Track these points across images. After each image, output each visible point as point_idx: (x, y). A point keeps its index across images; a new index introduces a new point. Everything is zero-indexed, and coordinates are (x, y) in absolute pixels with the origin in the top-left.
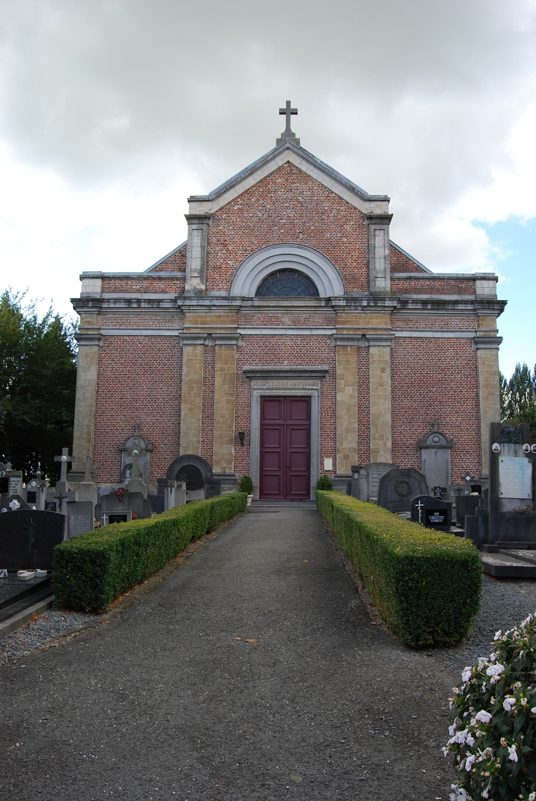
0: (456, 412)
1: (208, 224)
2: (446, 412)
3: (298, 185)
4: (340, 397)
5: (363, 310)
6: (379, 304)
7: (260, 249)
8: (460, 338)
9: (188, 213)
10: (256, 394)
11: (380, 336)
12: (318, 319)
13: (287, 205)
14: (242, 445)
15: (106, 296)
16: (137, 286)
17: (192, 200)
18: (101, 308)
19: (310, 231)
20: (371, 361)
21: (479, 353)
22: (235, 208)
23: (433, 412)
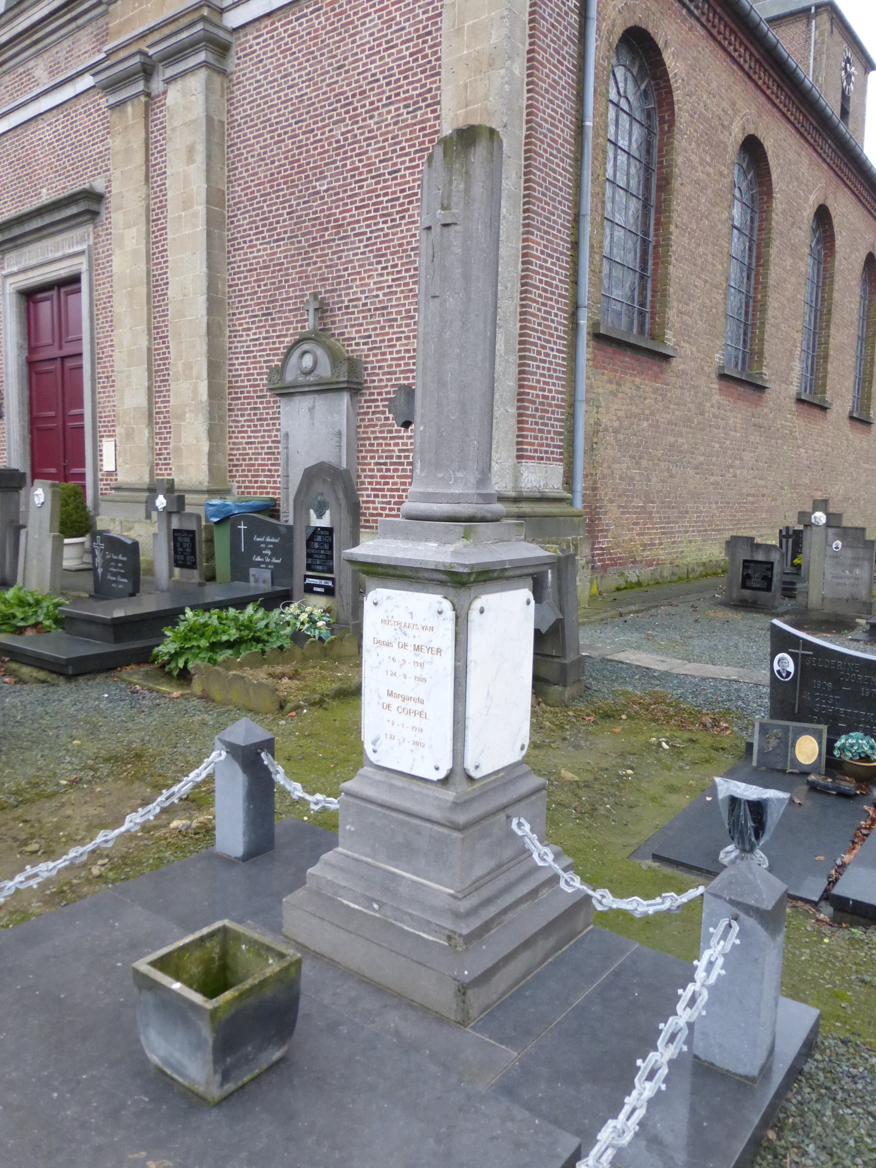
2: (352, 261)
23: (320, 268)
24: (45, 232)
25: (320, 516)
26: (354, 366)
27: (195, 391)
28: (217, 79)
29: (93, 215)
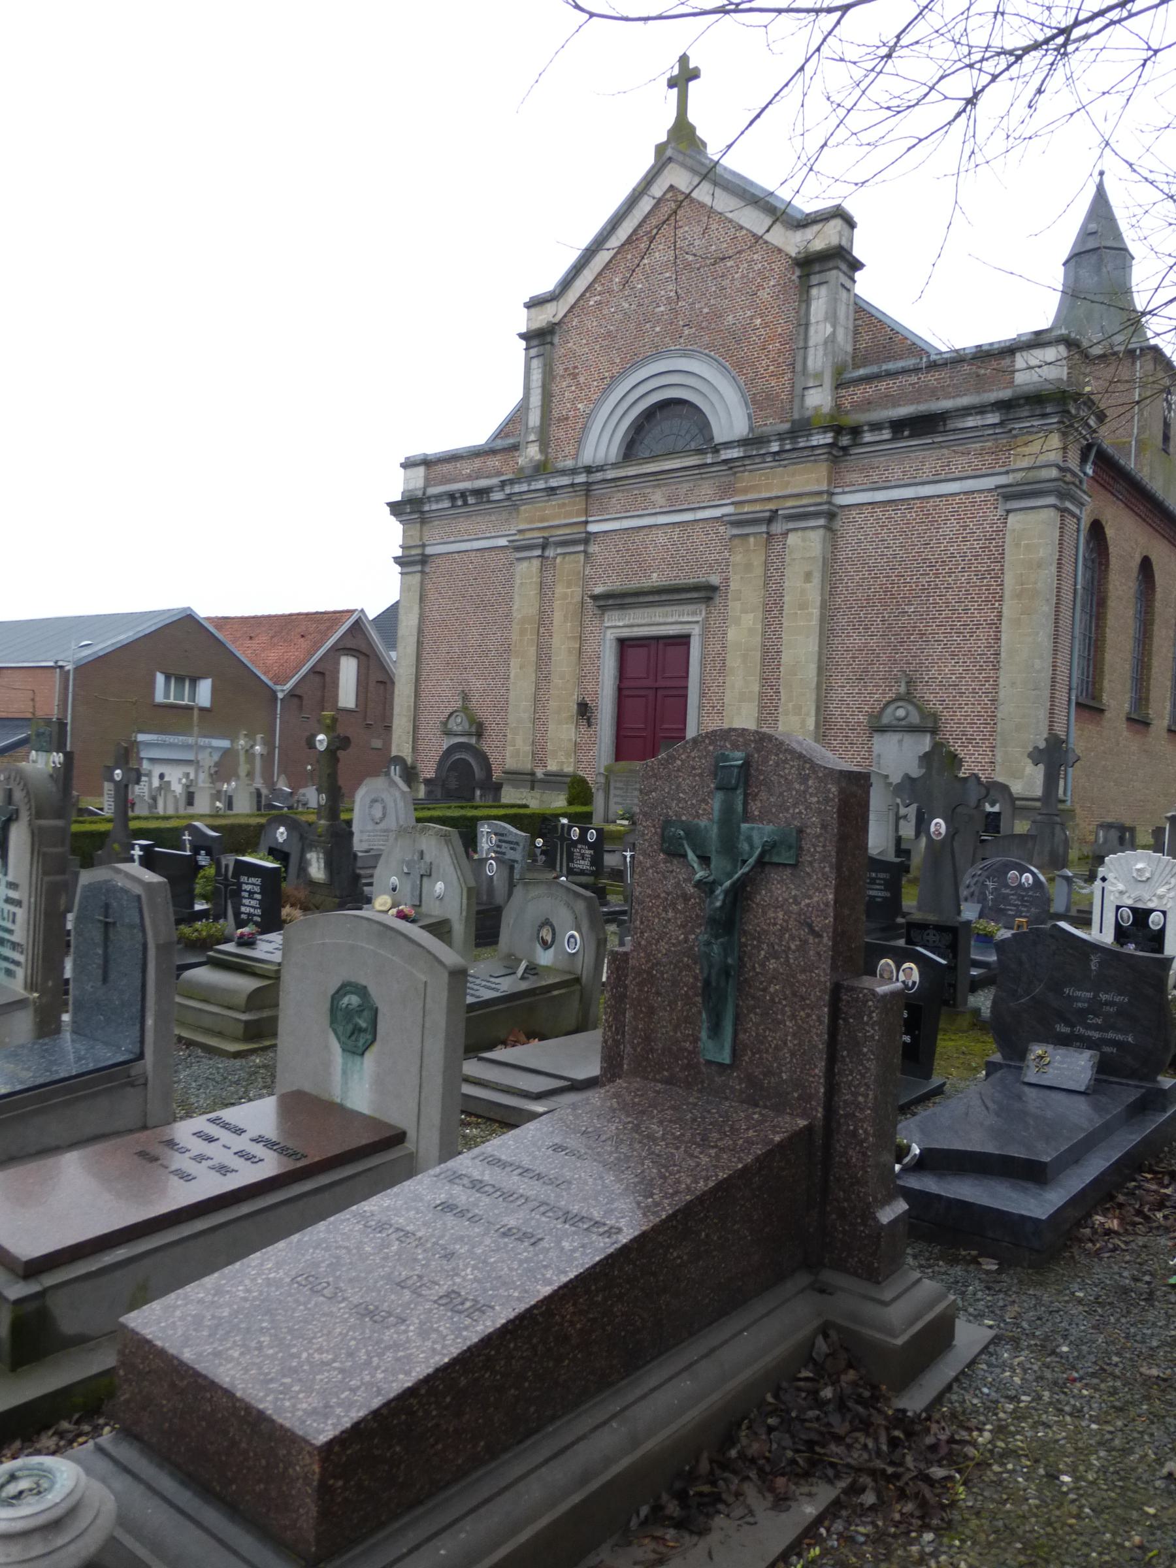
0: (953, 655)
1: (552, 344)
3: (687, 229)
4: (732, 634)
5: (775, 461)
6: (801, 445)
7: (624, 373)
8: (973, 492)
9: (524, 330)
10: (611, 635)
11: (801, 510)
12: (707, 489)
13: (667, 275)
14: (589, 725)
15: (433, 491)
16: (466, 468)
17: (534, 304)
18: (422, 512)
19: (701, 318)
20: (787, 558)
21: (1012, 518)
22: (592, 303)
24: (641, 599)
25: (992, 805)
26: (935, 717)
27: (803, 722)
28: (828, 534)
29: (710, 599)
